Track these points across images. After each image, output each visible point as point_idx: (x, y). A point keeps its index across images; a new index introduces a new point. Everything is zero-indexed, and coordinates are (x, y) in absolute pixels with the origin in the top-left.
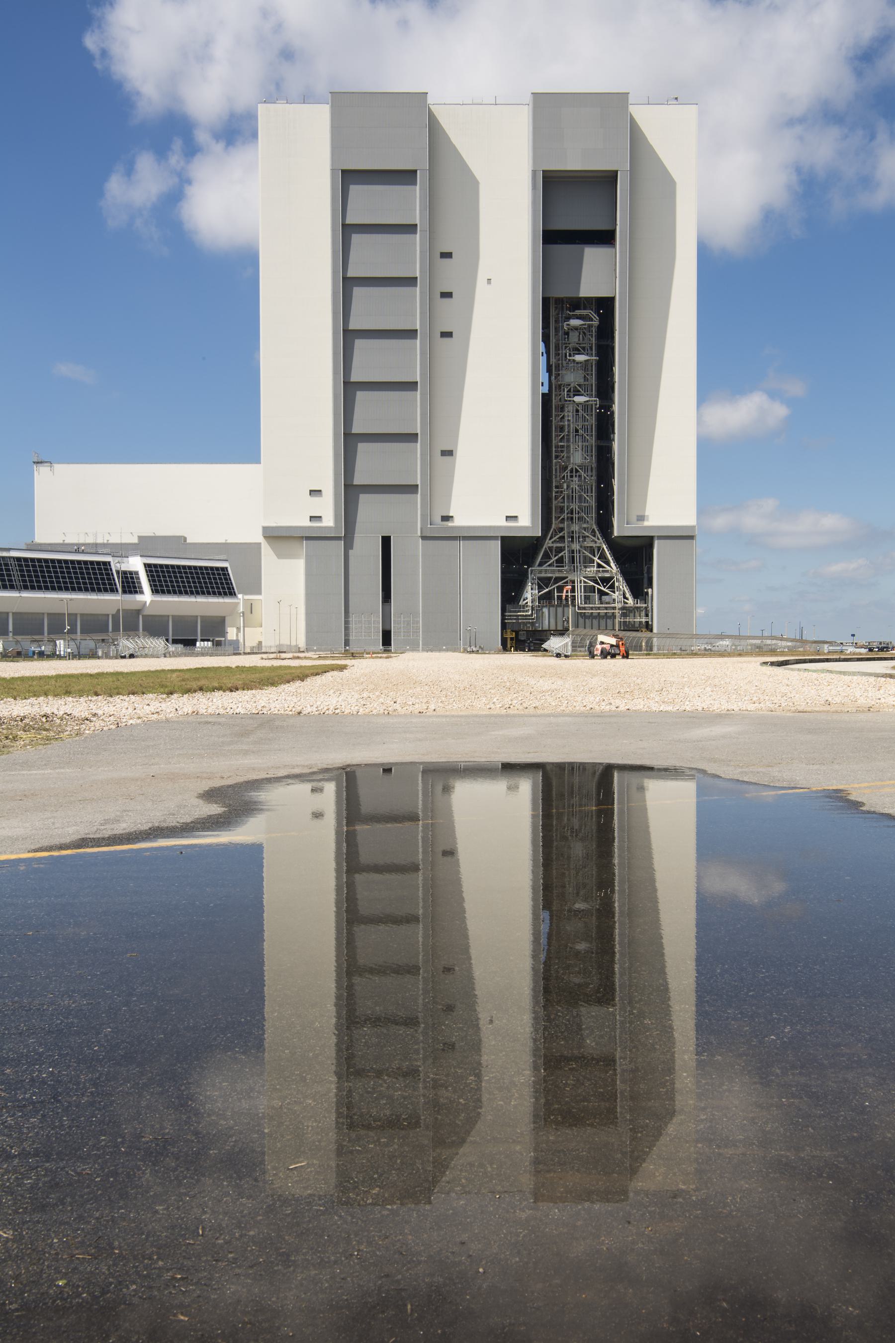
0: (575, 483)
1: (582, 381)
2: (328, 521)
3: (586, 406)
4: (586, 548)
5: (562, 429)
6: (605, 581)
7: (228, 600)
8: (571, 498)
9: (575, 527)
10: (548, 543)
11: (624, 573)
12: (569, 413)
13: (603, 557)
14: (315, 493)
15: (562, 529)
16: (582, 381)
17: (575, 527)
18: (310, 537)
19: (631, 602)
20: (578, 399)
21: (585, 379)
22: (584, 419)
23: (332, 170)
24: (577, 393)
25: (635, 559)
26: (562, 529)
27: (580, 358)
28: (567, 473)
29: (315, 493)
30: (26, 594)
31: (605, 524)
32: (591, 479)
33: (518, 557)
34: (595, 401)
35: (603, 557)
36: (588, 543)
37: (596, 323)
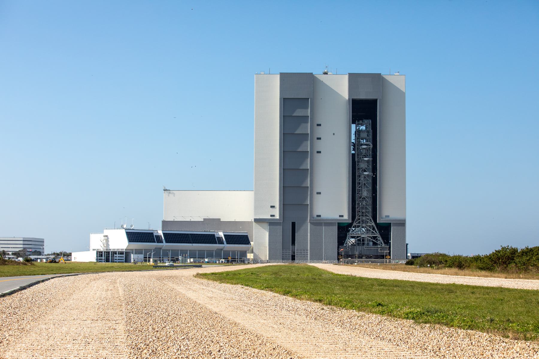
0: (364, 203)
1: (367, 167)
2: (277, 217)
3: (368, 175)
4: (368, 226)
5: (359, 183)
6: (375, 238)
7: (248, 246)
8: (363, 208)
9: (364, 218)
10: (354, 224)
11: (381, 235)
12: (362, 178)
13: (374, 229)
14: (272, 207)
15: (359, 219)
16: (367, 167)
17: (364, 218)
18: (271, 223)
19: (383, 245)
20: (365, 173)
21: (368, 166)
22: (368, 180)
23: (280, 99)
24: (365, 171)
25: (385, 230)
26: (359, 219)
27: (366, 159)
28: (361, 199)
29: (272, 207)
30: (194, 245)
31: (374, 218)
32: (370, 202)
33: (343, 230)
34: (371, 174)
35: (374, 229)
36: (369, 224)
37: (371, 147)
